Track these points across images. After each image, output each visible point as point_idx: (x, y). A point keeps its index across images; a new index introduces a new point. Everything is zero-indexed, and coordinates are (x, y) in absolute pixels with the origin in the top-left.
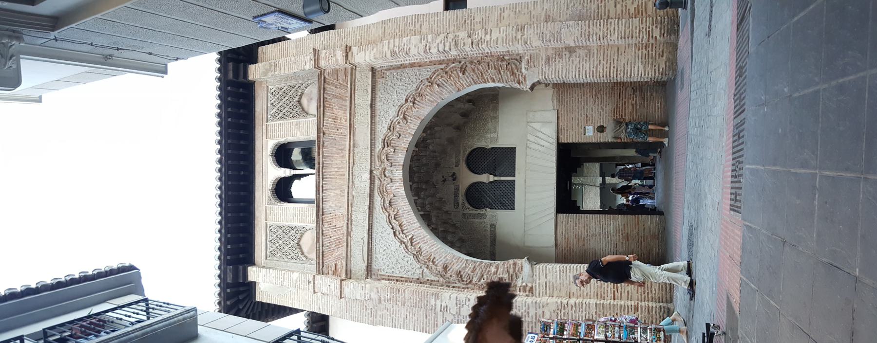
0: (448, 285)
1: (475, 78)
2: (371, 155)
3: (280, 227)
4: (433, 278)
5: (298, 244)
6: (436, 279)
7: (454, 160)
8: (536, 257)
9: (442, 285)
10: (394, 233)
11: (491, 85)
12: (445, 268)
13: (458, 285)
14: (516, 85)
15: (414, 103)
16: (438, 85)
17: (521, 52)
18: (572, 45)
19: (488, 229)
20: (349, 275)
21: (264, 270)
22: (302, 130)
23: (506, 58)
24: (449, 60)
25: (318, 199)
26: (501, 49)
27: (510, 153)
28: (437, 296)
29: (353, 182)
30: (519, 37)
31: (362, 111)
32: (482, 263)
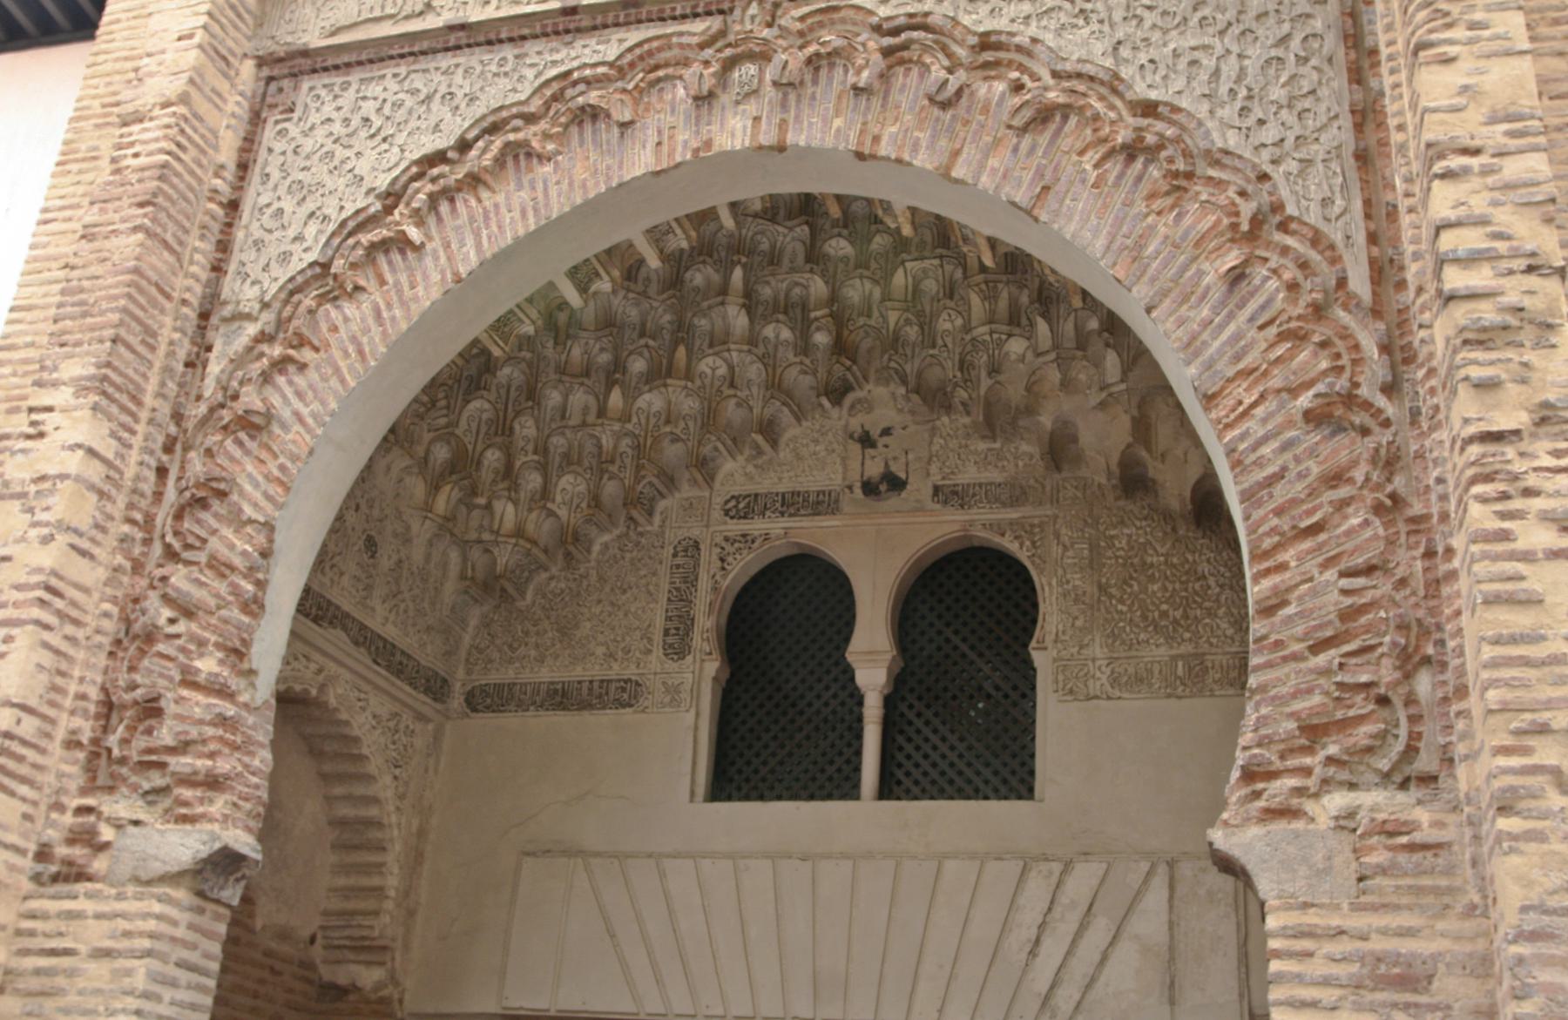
1: (1281, 493)
4: (215, 368)
6: (209, 388)
7: (969, 475)
9: (178, 417)
10: (439, 157)
12: (253, 425)
15: (1131, 151)
16: (1236, 277)
17: (1464, 778)
19: (616, 671)
23: (1424, 683)
24: (1402, 321)
27: (1007, 769)
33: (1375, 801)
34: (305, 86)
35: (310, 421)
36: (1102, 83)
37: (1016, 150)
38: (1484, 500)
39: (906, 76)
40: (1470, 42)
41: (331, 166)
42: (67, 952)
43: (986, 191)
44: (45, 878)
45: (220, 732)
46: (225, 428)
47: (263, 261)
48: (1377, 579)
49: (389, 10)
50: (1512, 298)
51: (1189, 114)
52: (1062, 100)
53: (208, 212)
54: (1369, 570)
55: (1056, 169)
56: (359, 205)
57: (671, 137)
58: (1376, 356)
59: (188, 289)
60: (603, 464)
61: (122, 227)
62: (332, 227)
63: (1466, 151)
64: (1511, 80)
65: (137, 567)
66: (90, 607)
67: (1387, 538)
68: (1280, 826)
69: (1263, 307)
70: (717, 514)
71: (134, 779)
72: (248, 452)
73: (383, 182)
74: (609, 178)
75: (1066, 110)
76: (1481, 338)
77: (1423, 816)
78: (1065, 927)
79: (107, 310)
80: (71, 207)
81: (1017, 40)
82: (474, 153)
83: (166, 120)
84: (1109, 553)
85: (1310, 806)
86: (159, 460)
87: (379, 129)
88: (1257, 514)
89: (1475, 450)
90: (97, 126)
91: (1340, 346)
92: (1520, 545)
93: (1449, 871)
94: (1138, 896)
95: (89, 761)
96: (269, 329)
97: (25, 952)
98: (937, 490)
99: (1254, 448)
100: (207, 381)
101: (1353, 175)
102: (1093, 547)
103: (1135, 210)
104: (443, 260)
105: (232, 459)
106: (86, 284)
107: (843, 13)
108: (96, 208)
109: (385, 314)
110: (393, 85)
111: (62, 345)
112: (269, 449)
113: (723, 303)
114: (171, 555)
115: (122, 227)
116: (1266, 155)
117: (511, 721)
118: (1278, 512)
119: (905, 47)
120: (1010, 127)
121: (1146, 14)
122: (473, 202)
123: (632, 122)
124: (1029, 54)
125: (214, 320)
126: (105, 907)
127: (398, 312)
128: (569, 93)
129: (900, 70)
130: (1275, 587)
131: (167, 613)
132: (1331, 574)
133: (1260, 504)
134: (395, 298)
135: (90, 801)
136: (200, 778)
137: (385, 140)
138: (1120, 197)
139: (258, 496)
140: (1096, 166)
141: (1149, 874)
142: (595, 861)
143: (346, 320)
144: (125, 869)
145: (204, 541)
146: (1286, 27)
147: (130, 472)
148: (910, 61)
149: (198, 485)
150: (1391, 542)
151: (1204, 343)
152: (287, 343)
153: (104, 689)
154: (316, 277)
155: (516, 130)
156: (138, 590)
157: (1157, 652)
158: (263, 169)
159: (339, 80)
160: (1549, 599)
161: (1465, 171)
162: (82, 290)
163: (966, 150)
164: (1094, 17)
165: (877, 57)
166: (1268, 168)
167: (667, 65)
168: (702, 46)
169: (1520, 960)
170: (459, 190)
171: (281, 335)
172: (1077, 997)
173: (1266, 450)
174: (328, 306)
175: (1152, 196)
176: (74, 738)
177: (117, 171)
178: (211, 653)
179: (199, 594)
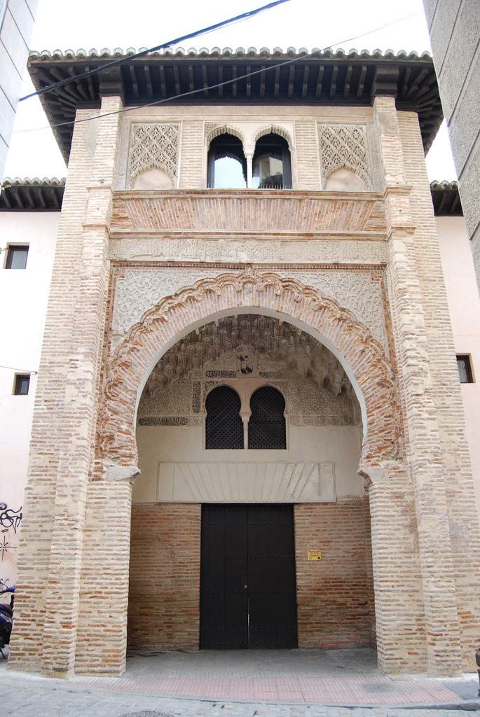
0: (104, 368)
2: (271, 265)
3: (175, 142)
4: (113, 349)
5: (153, 166)
6: (112, 353)
7: (268, 370)
9: (103, 360)
10: (170, 297)
11: (365, 419)
12: (126, 365)
13: (105, 381)
14: (365, 453)
15: (340, 320)
16: (363, 351)
17: (408, 459)
18: (420, 529)
19: (180, 415)
20: (114, 237)
22: (306, 171)
23: (400, 439)
24: (395, 364)
25: (213, 192)
26: (412, 433)
29: (236, 240)
30: (427, 456)
32: (133, 412)
33: (393, 463)
34: (127, 270)
37: (314, 315)
38: (416, 407)
40: (412, 310)
42: (103, 498)
47: (123, 320)
48: (391, 418)
49: (150, 254)
50: (420, 366)
54: (390, 416)
60: (177, 362)
62: (142, 313)
63: (412, 334)
64: (419, 319)
65: (99, 401)
68: (375, 467)
70: (204, 375)
72: (126, 372)
73: (156, 303)
75: (325, 307)
76: (415, 374)
77: (400, 465)
80: (59, 297)
82: (180, 298)
85: (380, 463)
89: (414, 397)
91: (383, 369)
92: (422, 417)
93: (406, 476)
94: (312, 471)
96: (128, 339)
97: (92, 498)
98: (260, 373)
99: (367, 389)
102: (298, 390)
104: (174, 326)
105: (122, 374)
109: (160, 338)
111: (77, 342)
114: (109, 398)
117: (152, 428)
118: (372, 403)
119: (288, 286)
124: (316, 292)
125: (109, 335)
127: (163, 337)
128: (204, 285)
129: (286, 291)
130: (372, 420)
131: (110, 413)
132: (383, 417)
133: (368, 401)
135: (99, 461)
138: (338, 329)
141: (314, 467)
142: (179, 464)
147: (96, 376)
150: (393, 411)
152: (133, 344)
157: (314, 415)
160: (428, 427)
161: (412, 338)
162: (80, 327)
168: (237, 278)
169: (423, 494)
177: (83, 293)
179: (118, 409)
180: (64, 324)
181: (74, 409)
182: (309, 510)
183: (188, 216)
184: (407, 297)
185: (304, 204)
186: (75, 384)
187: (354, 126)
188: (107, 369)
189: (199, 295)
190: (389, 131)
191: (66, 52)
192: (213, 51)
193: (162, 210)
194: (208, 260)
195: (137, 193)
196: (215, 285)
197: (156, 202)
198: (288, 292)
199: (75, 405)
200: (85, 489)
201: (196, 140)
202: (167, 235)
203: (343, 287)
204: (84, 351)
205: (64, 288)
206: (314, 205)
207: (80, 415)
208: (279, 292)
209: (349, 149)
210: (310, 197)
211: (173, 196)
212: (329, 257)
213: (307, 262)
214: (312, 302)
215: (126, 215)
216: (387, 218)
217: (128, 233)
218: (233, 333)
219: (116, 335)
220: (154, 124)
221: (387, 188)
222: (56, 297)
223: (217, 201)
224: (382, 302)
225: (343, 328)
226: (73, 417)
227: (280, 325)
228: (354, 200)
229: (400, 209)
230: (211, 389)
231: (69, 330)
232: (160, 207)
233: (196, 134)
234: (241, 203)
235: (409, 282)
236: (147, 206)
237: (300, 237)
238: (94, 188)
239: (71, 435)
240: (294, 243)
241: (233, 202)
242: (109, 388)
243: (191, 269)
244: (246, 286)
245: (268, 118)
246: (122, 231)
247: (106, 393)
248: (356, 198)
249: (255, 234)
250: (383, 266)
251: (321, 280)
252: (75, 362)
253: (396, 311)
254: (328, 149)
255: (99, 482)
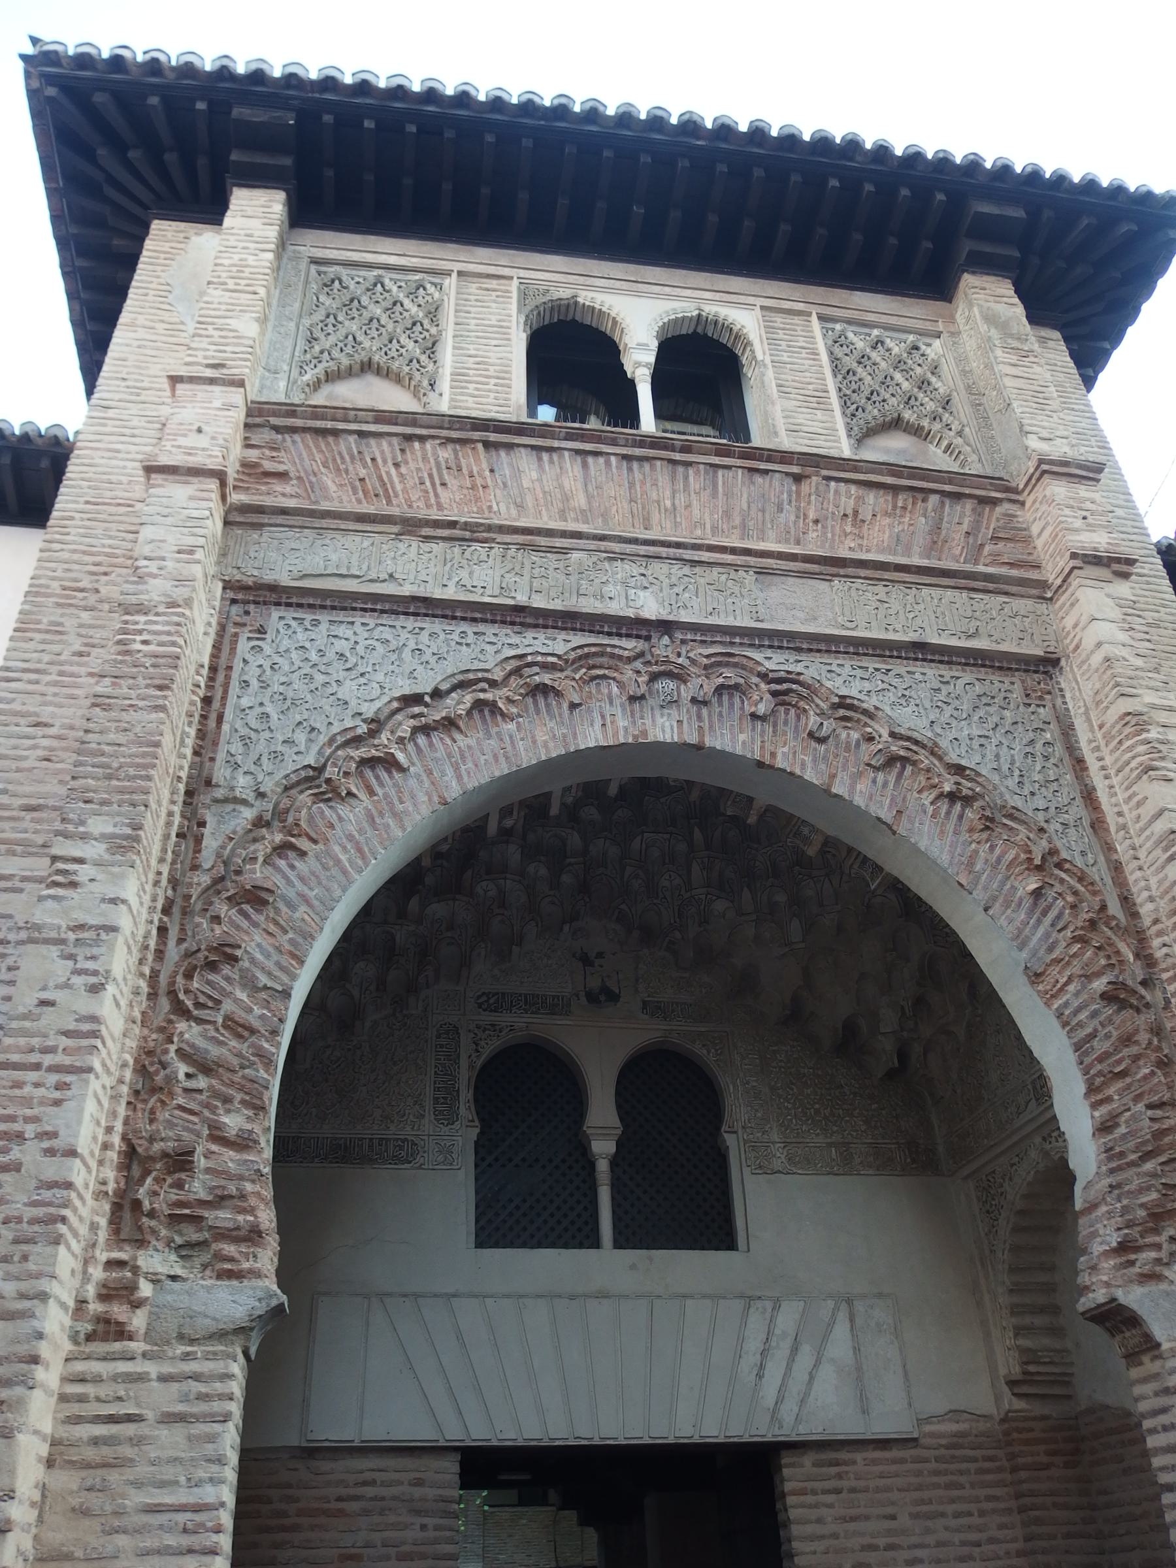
0: (175, 906)
1: (1100, 1046)
3: (434, 313)
4: (210, 843)
5: (367, 367)
6: (207, 858)
8: (278, 1353)
9: (174, 882)
11: (1075, 1116)
12: (256, 898)
13: (173, 952)
15: (952, 797)
16: (1037, 894)
20: (242, 519)
21: (272, 233)
28: (125, 845)
29: (622, 557)
31: (895, 606)
35: (316, 903)
36: (924, 747)
37: (874, 781)
39: (787, 713)
41: (312, 687)
42: (130, 1419)
43: (859, 807)
44: (82, 1336)
45: (257, 1188)
46: (229, 899)
51: (987, 779)
52: (902, 753)
53: (192, 703)
55: (904, 799)
56: (349, 724)
57: (612, 723)
58: (1132, 960)
59: (181, 768)
61: (141, 704)
62: (323, 739)
66: (114, 1057)
67: (1167, 1084)
69: (1059, 917)
71: (164, 1232)
72: (255, 925)
73: (369, 710)
74: (566, 744)
75: (904, 760)
78: (781, 1352)
79: (135, 777)
80: (37, 671)
81: (865, 706)
82: (449, 701)
83: (176, 619)
84: (774, 1064)
86: (160, 920)
87: (356, 665)
88: (1087, 1060)
90: (58, 605)
91: (1110, 951)
95: (113, 1213)
96: (268, 816)
97: (77, 1420)
100: (204, 853)
101: (1094, 839)
103: (962, 839)
104: (427, 784)
105: (238, 928)
106: (106, 748)
107: (736, 660)
108: (107, 681)
109: (378, 820)
110: (363, 633)
112: (276, 923)
113: (507, 842)
114: (181, 1011)
115: (141, 704)
116: (1041, 816)
118: (1100, 1059)
119: (786, 692)
120: (868, 765)
121: (944, 706)
122: (448, 741)
123: (580, 705)
124: (871, 716)
125: (205, 798)
126: (167, 1369)
129: (782, 709)
130: (1110, 1112)
131: (182, 1069)
133: (1086, 1053)
134: (386, 807)
135: (123, 1256)
136: (242, 1233)
137: (362, 675)
138: (950, 827)
139: (270, 965)
140: (932, 803)
143: (340, 818)
144: (170, 1326)
145: (218, 1002)
146: (1031, 735)
148: (789, 704)
149: (211, 949)
151: (1027, 937)
152: (282, 830)
153: (124, 1138)
154: (308, 779)
155: (483, 690)
156: (152, 1044)
158: (240, 676)
159: (308, 617)
163: (839, 775)
164: (913, 702)
165: (768, 696)
166: (1045, 826)
167: (601, 667)
168: (629, 660)
170: (435, 729)
171: (276, 823)
172: (796, 1409)
173: (1082, 1016)
174: (321, 805)
175: (971, 830)
176: (103, 1188)
177: (127, 652)
178: (238, 1111)
179: (215, 1052)
180: (41, 753)
181: (45, 1036)
182: (833, 1470)
183: (473, 487)
184: (1153, 734)
185: (805, 487)
186: (63, 942)
187: (911, 338)
188: (185, 912)
189: (510, 701)
190: (1015, 344)
191: (145, 53)
192: (556, 102)
193: (397, 465)
194: (539, 602)
195: (317, 412)
196: (561, 675)
197: (379, 445)
198: (787, 713)
199: (50, 1020)
200: (49, 1376)
201: (493, 317)
202: (410, 526)
203: (948, 711)
204: (110, 829)
205: (56, 648)
206: (836, 492)
207: (67, 1060)
208: (762, 709)
209: (906, 385)
210: (825, 472)
211: (432, 432)
212: (899, 627)
213: (836, 632)
214: (864, 746)
215: (281, 468)
216: (1039, 543)
217: (284, 511)
218: (566, 878)
219: (226, 800)
220: (376, 272)
221: (1041, 462)
222: (25, 671)
223: (561, 457)
224: (1067, 759)
225: (965, 826)
226: (37, 1067)
227: (752, 820)
228: (942, 493)
229: (1084, 513)
230: (489, 1048)
231: (57, 772)
232: (389, 456)
233: (494, 305)
234: (630, 469)
235: (1150, 698)
236: (349, 450)
237: (808, 565)
238: (192, 380)
239: (20, 1137)
240: (791, 580)
241: (608, 464)
242: (189, 976)
243: (481, 627)
244: (659, 685)
245: (688, 293)
246: (268, 501)
247: (172, 993)
248: (947, 488)
249: (678, 545)
250: (1047, 665)
251: (881, 686)
252: (75, 867)
253: (1115, 781)
254: (850, 377)
255: (117, 1346)
